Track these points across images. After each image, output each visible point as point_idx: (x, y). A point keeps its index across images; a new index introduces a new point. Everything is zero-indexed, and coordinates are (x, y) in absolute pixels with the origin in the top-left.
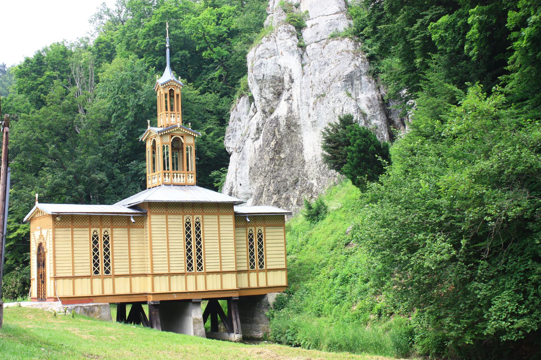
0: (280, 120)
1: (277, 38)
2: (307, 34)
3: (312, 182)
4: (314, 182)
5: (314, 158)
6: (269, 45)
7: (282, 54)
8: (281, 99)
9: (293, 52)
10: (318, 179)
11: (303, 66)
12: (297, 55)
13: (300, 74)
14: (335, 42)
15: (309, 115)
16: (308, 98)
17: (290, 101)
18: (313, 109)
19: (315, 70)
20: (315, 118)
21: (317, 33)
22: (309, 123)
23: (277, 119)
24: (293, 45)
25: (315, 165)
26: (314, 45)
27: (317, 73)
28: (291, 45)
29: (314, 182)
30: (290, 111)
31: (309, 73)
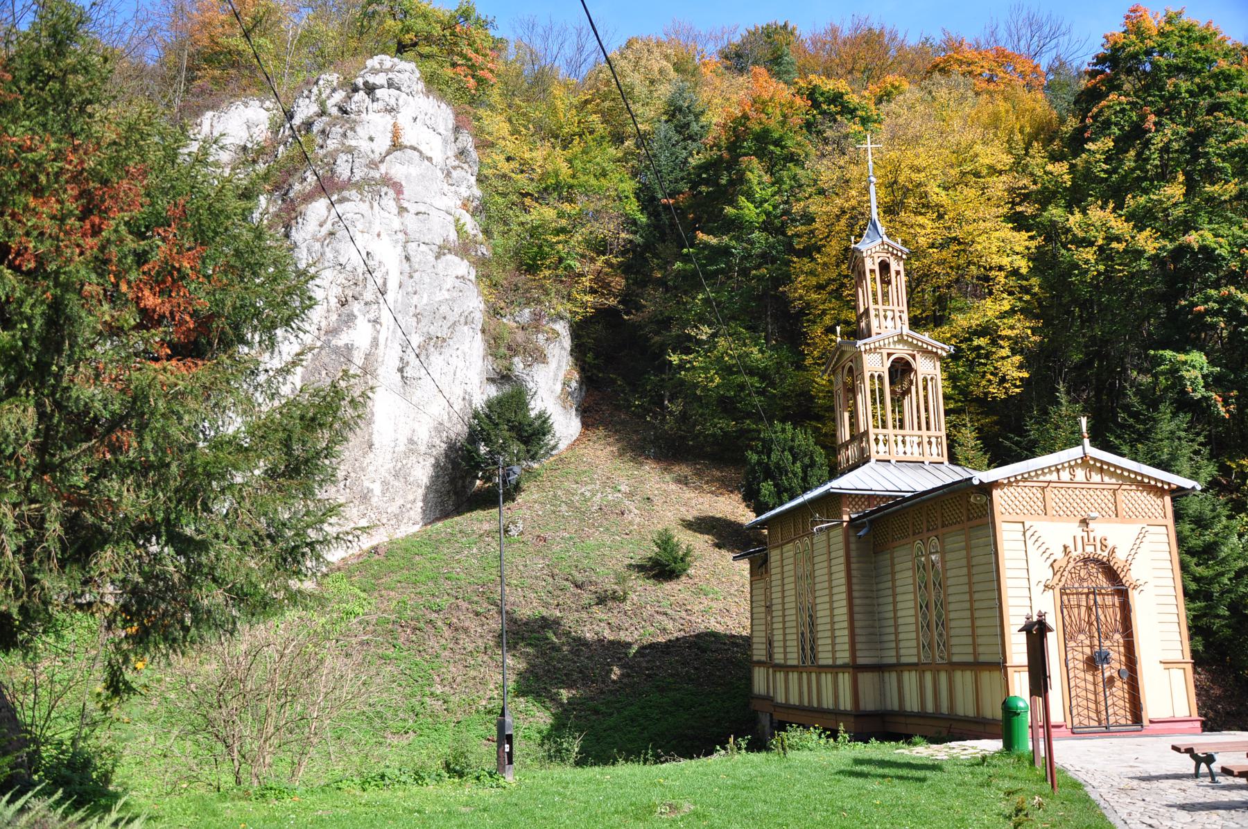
0: (355, 353)
1: (375, 204)
3: (371, 486)
4: (377, 488)
5: (393, 444)
6: (364, 207)
7: (379, 235)
8: (355, 317)
9: (397, 242)
10: (385, 483)
17: (378, 326)
23: (349, 348)
25: (389, 456)
27: (425, 296)
29: (377, 488)
30: (375, 343)
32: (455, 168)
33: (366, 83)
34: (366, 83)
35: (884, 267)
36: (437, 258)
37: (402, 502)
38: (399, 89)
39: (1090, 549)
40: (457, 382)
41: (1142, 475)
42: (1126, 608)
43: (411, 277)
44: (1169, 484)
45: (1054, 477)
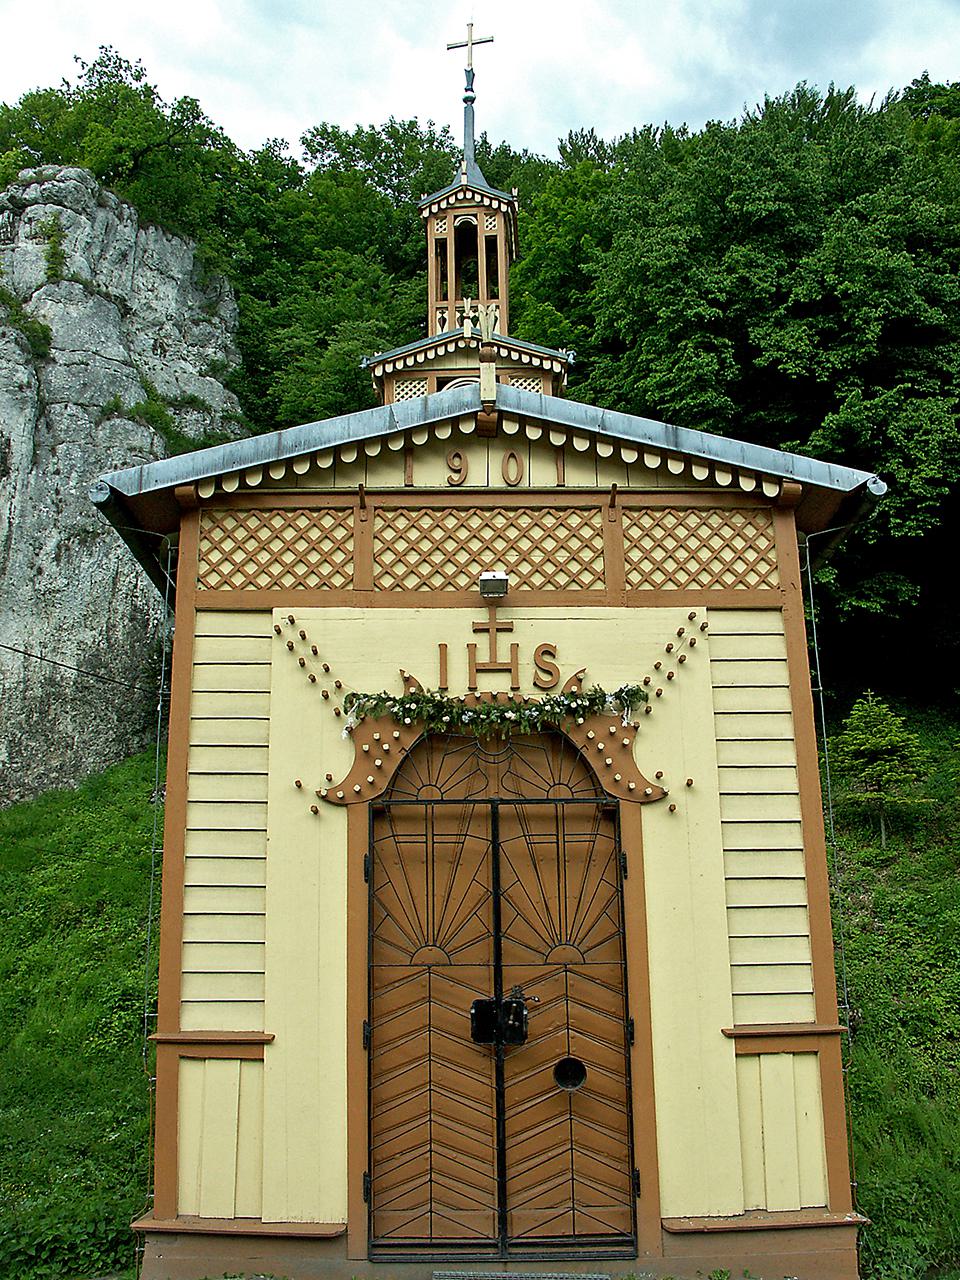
2: (56, 376)
9: (24, 401)
11: (36, 446)
12: (29, 412)
13: (25, 462)
14: (130, 425)
15: (40, 571)
16: (41, 527)
18: (57, 559)
19: (73, 467)
20: (61, 582)
21: (85, 384)
22: (26, 591)
24: (29, 385)
25: (17, 705)
26: (72, 409)
28: (25, 381)
31: (51, 468)
32: (196, 323)
33: (12, 199)
34: (12, 199)
35: (466, 235)
36: (97, 424)
37: (42, 769)
38: (60, 204)
39: (494, 684)
40: (120, 596)
41: (689, 460)
42: (621, 866)
43: (53, 451)
44: (778, 480)
45: (393, 479)
